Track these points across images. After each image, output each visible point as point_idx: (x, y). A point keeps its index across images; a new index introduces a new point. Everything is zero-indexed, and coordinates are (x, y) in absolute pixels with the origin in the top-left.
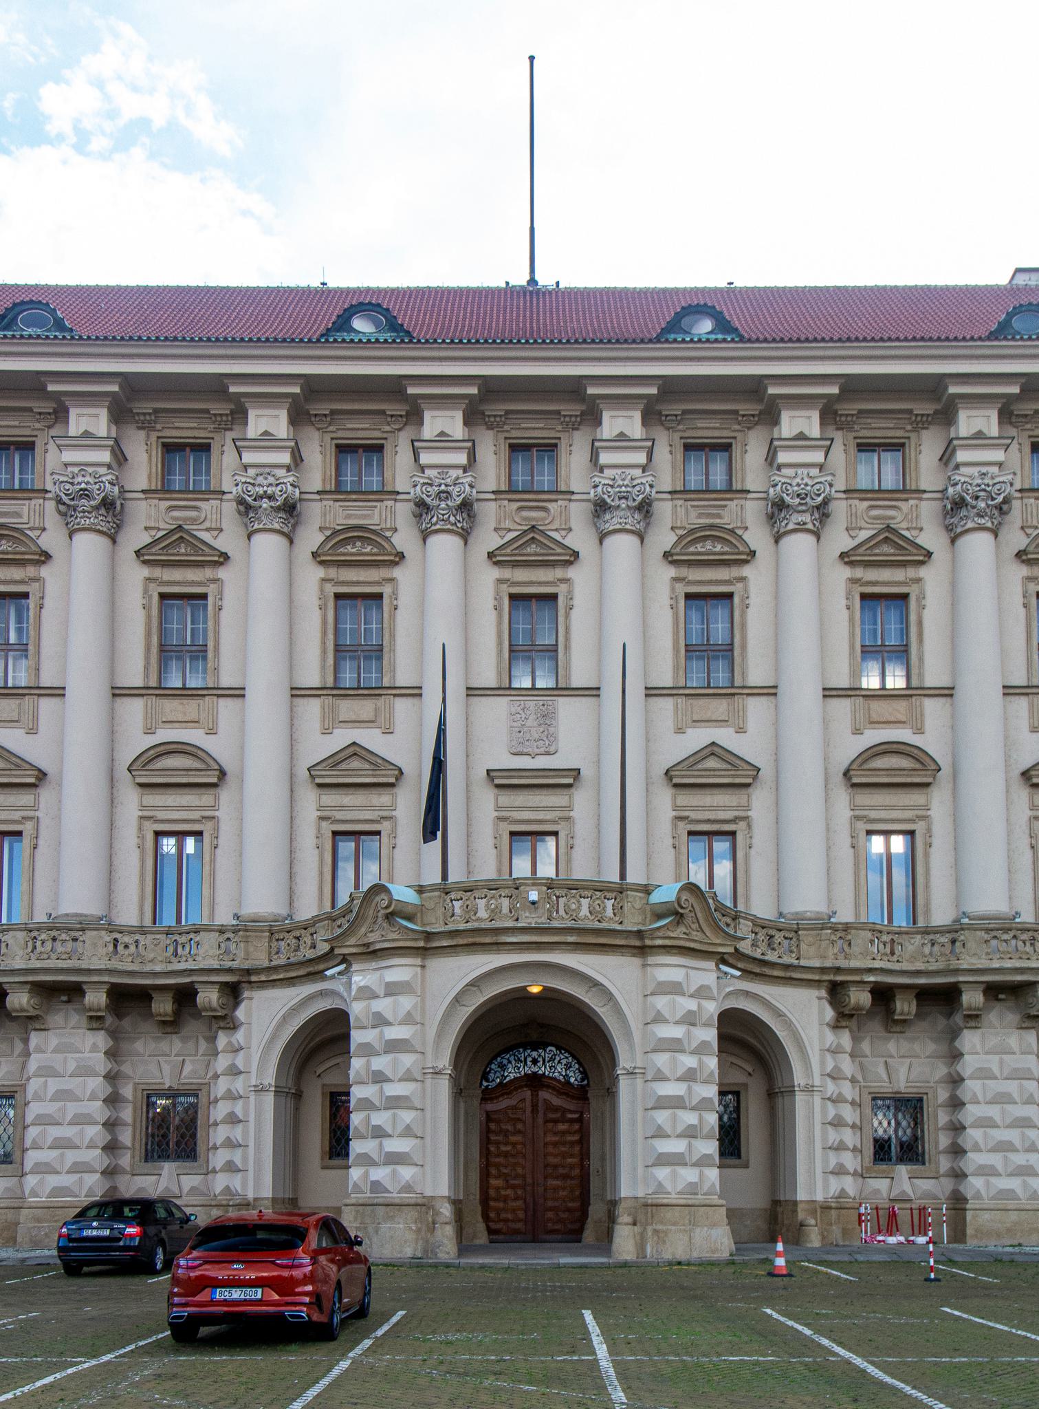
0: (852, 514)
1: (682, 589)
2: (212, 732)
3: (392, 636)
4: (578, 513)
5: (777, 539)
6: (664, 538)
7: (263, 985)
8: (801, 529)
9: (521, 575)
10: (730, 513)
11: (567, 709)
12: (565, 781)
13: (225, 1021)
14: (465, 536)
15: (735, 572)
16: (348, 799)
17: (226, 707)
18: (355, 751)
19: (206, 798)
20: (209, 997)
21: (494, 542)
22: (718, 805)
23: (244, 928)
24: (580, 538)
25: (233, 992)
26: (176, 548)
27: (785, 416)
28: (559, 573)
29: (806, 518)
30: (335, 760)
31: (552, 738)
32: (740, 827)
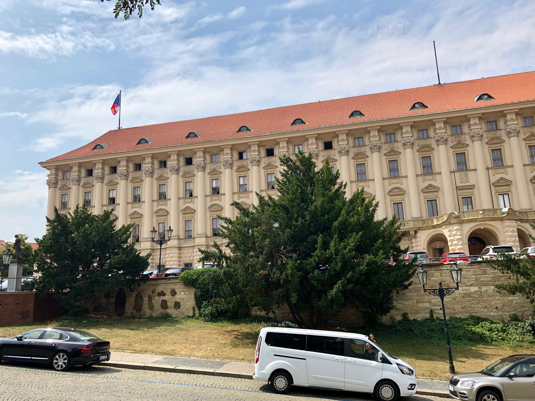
0: (524, 131)
1: (490, 149)
2: (401, 184)
3: (434, 163)
4: (467, 137)
5: (509, 138)
6: (486, 140)
7: (422, 230)
8: (514, 136)
9: (457, 150)
10: (498, 133)
11: (470, 173)
12: (472, 187)
13: (415, 237)
14: (446, 144)
15: (501, 145)
16: (429, 194)
17: (404, 180)
18: (430, 185)
19: (402, 197)
20: (412, 233)
21: (452, 145)
22: (504, 189)
23: (415, 220)
24: (468, 142)
25: (416, 232)
26: (393, 152)
27: (508, 116)
28: (465, 149)
29: (515, 134)
30: (426, 188)
31: (468, 179)
32: (509, 193)
